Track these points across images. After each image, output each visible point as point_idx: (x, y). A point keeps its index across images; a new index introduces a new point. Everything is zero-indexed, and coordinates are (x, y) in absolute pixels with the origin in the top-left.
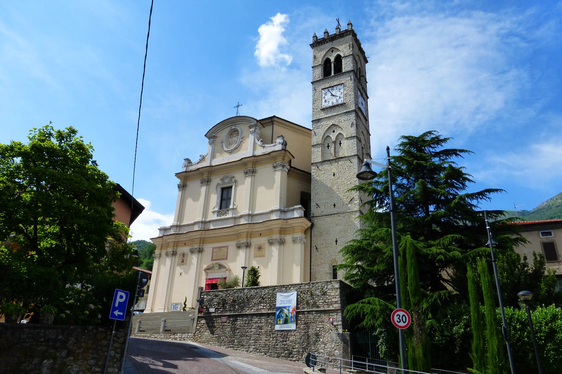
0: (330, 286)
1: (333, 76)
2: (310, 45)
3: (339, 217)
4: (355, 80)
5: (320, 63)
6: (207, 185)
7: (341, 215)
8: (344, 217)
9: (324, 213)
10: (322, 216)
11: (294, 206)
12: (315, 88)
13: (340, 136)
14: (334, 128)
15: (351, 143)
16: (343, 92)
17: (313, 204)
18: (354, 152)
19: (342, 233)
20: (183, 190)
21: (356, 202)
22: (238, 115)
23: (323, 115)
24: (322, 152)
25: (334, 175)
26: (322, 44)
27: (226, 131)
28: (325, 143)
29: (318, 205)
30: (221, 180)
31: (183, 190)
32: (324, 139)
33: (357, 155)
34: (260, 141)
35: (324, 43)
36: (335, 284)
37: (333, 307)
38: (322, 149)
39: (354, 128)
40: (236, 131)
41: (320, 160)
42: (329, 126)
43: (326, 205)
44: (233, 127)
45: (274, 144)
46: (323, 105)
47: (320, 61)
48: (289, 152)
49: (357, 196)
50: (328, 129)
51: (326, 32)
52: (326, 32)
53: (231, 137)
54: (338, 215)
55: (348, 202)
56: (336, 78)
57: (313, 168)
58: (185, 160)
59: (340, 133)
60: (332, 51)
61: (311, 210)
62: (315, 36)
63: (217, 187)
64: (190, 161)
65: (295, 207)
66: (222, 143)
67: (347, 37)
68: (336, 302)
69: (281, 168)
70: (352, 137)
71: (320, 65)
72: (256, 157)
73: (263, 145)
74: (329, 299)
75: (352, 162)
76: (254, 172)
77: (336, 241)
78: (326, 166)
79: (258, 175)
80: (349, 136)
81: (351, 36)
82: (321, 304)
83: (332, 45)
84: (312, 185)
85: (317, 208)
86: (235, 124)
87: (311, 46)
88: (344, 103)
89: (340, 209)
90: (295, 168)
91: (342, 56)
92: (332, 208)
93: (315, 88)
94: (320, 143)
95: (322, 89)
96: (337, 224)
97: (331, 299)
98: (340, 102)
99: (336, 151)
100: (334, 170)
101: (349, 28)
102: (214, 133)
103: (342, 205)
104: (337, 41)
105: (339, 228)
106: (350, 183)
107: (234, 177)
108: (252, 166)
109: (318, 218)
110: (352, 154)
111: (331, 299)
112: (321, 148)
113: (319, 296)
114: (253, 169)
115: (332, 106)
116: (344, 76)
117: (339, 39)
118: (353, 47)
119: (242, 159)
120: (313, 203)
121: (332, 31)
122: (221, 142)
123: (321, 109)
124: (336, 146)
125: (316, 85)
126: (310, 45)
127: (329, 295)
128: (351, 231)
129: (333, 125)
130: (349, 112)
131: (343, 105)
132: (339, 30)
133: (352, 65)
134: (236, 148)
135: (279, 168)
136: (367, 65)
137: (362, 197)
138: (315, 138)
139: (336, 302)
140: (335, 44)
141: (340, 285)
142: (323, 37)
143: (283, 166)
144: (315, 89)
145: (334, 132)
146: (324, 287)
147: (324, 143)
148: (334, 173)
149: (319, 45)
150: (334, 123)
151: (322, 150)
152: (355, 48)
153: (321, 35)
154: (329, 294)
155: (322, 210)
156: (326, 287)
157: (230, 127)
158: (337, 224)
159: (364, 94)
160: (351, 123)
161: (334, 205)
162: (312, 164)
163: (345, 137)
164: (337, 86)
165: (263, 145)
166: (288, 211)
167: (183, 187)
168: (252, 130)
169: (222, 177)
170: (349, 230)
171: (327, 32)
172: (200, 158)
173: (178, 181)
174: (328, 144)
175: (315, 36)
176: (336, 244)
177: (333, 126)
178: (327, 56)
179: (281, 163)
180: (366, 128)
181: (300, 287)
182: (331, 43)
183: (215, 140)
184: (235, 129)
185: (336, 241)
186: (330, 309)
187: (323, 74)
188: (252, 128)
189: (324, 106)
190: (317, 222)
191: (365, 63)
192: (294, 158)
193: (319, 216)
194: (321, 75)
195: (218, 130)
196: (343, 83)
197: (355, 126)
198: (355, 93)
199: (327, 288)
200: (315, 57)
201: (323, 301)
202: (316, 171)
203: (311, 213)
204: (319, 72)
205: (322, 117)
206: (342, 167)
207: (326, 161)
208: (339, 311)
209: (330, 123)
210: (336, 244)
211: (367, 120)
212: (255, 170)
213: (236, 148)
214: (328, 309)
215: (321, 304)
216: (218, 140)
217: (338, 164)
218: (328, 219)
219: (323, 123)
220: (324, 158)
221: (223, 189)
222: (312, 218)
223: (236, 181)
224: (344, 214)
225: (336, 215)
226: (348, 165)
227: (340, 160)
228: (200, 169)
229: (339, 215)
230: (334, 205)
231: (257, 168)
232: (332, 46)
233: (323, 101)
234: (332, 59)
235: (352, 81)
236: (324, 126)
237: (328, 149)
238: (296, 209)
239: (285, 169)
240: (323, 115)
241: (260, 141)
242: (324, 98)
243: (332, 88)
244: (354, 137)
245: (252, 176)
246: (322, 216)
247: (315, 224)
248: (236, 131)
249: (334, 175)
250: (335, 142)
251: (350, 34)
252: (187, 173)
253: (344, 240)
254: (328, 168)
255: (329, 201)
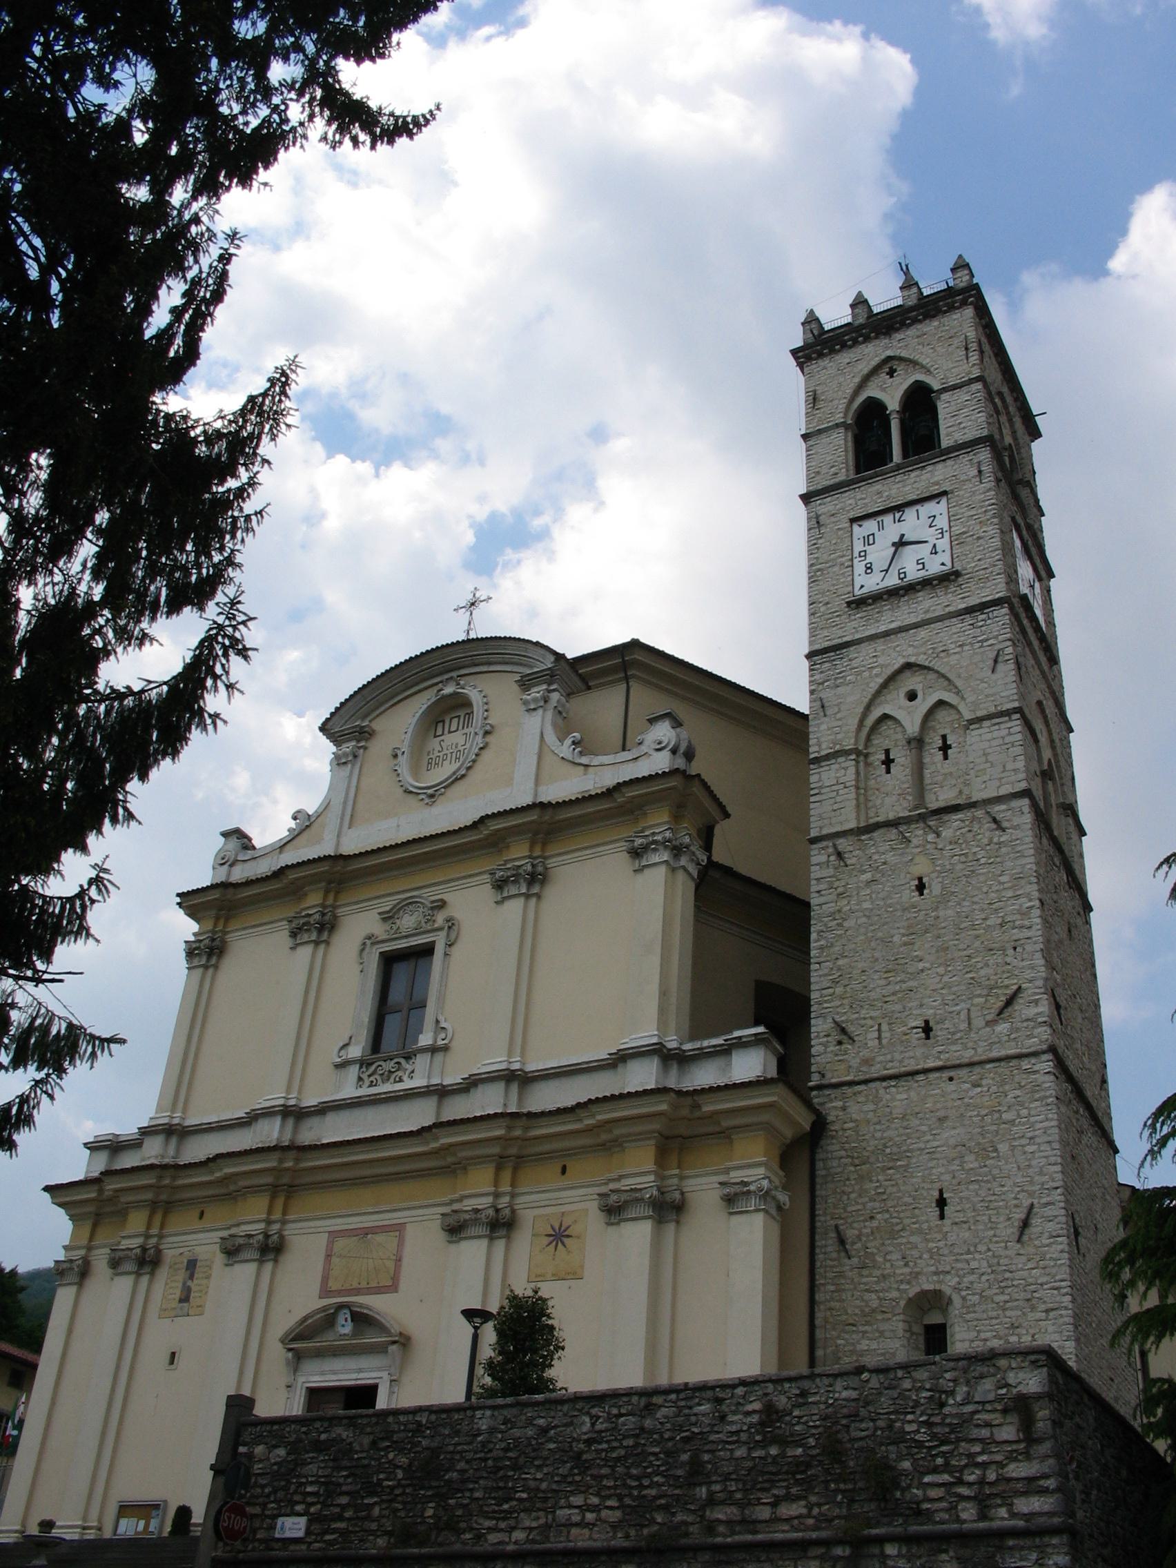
0: (986, 1388)
1: (898, 467)
2: (794, 352)
3: (951, 1087)
4: (998, 481)
5: (839, 418)
6: (317, 943)
7: (963, 1073)
8: (976, 1085)
9: (877, 1070)
10: (866, 1082)
11: (731, 1032)
12: (817, 517)
13: (943, 715)
14: (912, 681)
15: (995, 743)
16: (946, 528)
17: (819, 1026)
18: (1013, 778)
19: (971, 1162)
20: (206, 967)
21: (1032, 1011)
22: (472, 635)
23: (855, 626)
24: (857, 788)
25: (921, 887)
26: (844, 346)
27: (419, 704)
28: (871, 750)
29: (843, 1031)
30: (384, 920)
31: (206, 967)
32: (866, 730)
33: (1026, 793)
34: (568, 741)
35: (855, 343)
36: (1021, 1375)
37: (1013, 1515)
38: (858, 773)
39: (1007, 670)
40: (460, 704)
41: (852, 825)
42: (889, 671)
43: (885, 1027)
44: (449, 689)
45: (634, 753)
46: (857, 587)
47: (838, 409)
48: (705, 785)
49: (1040, 983)
50: (885, 685)
51: (860, 303)
52: (860, 303)
53: (439, 732)
54: (946, 1074)
55: (995, 1011)
56: (913, 474)
57: (818, 856)
58: (226, 834)
59: (941, 703)
60: (891, 373)
61: (810, 1056)
62: (811, 320)
63: (362, 950)
64: (250, 840)
65: (737, 1034)
66: (395, 756)
67: (956, 315)
68: (1031, 1486)
69: (665, 856)
70: (1002, 714)
71: (837, 426)
72: (550, 812)
73: (584, 760)
74: (984, 1465)
75: (1005, 824)
76: (537, 879)
77: (941, 1203)
78: (882, 847)
79: (552, 893)
80: (984, 713)
81: (969, 312)
82: (933, 1493)
83: (887, 348)
84: (813, 936)
85: (840, 1043)
86: (454, 674)
87: (796, 358)
88: (957, 574)
89: (954, 1048)
90: (728, 871)
91: (936, 386)
92: (915, 1042)
93: (817, 517)
94: (849, 744)
95: (853, 520)
96: (942, 1120)
97: (1001, 1465)
98: (935, 567)
99: (927, 781)
100: (921, 867)
101: (962, 280)
102: (364, 718)
103: (963, 1026)
104: (912, 332)
105: (951, 1135)
106: (1000, 921)
107: (442, 905)
108: (531, 849)
109: (849, 1091)
110: (1003, 792)
111: (1001, 1465)
112: (852, 770)
113: (920, 1445)
114: (533, 866)
115: (901, 588)
116: (949, 462)
117: (919, 326)
118: (982, 352)
119: (483, 819)
120: (820, 1021)
121: (886, 296)
122: (389, 752)
123: (849, 604)
124: (926, 760)
125: (826, 506)
126: (794, 352)
127: (981, 1441)
128: (1013, 1148)
129: (908, 666)
130: (982, 607)
131: (948, 578)
132: (915, 290)
133: (982, 417)
134: (457, 778)
135: (655, 858)
136: (1036, 446)
137: (1058, 991)
138: (824, 727)
139: (1031, 1486)
140: (902, 344)
141: (1052, 1380)
142: (849, 319)
143: (677, 851)
144: (816, 523)
145: (912, 696)
146: (952, 1393)
147: (866, 747)
148: (920, 879)
149: (833, 351)
150: (912, 660)
151: (857, 780)
152: (986, 354)
153: (835, 314)
154: (985, 1433)
155: (865, 1053)
156: (962, 1391)
157: (435, 689)
158: (942, 1120)
159: (1033, 550)
160: (992, 655)
161: (927, 1029)
162: (813, 841)
163: (968, 715)
164: (918, 507)
165: (584, 760)
166: (702, 1055)
167: (210, 955)
168: (537, 692)
169: (387, 904)
170: (1004, 1148)
171: (866, 301)
172: (293, 824)
173: (188, 928)
174: (887, 752)
175: (811, 320)
176: (942, 1217)
177: (908, 673)
178: (872, 391)
179: (668, 834)
180: (1053, 693)
181: (804, 1394)
182: (884, 341)
183: (365, 748)
184: (455, 694)
185: (941, 1203)
186: (996, 1524)
187: (851, 463)
188: (536, 689)
189: (864, 590)
190: (844, 1109)
191: (1027, 438)
192: (727, 815)
193: (851, 1084)
194: (847, 463)
195: (382, 704)
196: (945, 493)
197: (1011, 665)
198: (1002, 532)
199: (967, 1400)
200: (814, 399)
201: (946, 1477)
202: (831, 871)
203: (813, 1068)
204: (838, 447)
205: (857, 636)
206: (957, 851)
207: (878, 826)
208: (1055, 1541)
209: (892, 656)
210: (942, 1217)
211: (1053, 660)
212: (540, 869)
213: (457, 778)
214: (981, 1525)
215: (933, 1493)
216: (379, 748)
217: (938, 835)
218: (899, 1097)
219: (860, 656)
220: (871, 814)
221: (390, 961)
222: (814, 1093)
223: (451, 923)
224: (977, 1069)
225: (937, 1075)
226: (985, 841)
227: (946, 817)
228: (288, 872)
229: (952, 1074)
230: (927, 1029)
231: (551, 863)
232: (889, 353)
233: (859, 567)
234: (892, 400)
235: (989, 481)
236: (866, 674)
237: (888, 772)
238: (741, 1044)
239: (684, 861)
240: (855, 626)
241: (568, 741)
242: (864, 554)
243: (898, 515)
244: (1007, 713)
245: (527, 896)
246: (866, 1082)
247: (830, 1118)
248: (460, 704)
249: (921, 887)
250: (918, 743)
251: (964, 303)
252: (231, 890)
253: (983, 1193)
254: (890, 857)
255: (898, 1007)
